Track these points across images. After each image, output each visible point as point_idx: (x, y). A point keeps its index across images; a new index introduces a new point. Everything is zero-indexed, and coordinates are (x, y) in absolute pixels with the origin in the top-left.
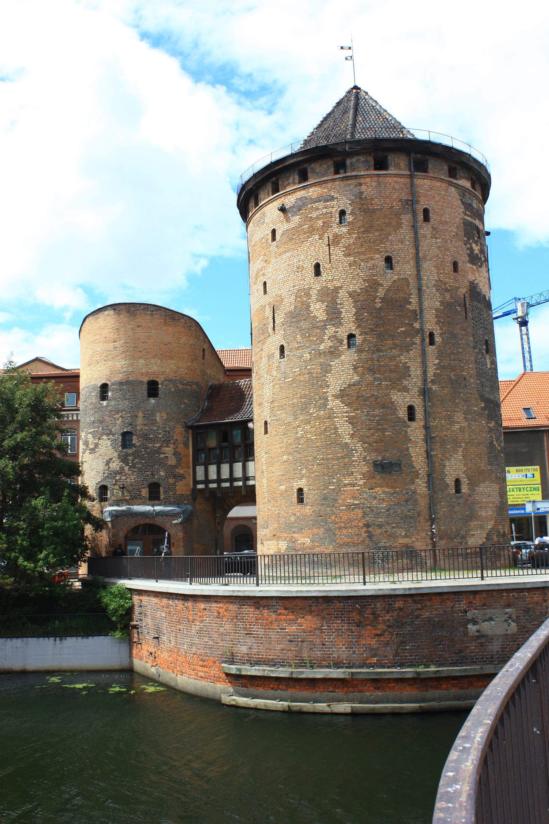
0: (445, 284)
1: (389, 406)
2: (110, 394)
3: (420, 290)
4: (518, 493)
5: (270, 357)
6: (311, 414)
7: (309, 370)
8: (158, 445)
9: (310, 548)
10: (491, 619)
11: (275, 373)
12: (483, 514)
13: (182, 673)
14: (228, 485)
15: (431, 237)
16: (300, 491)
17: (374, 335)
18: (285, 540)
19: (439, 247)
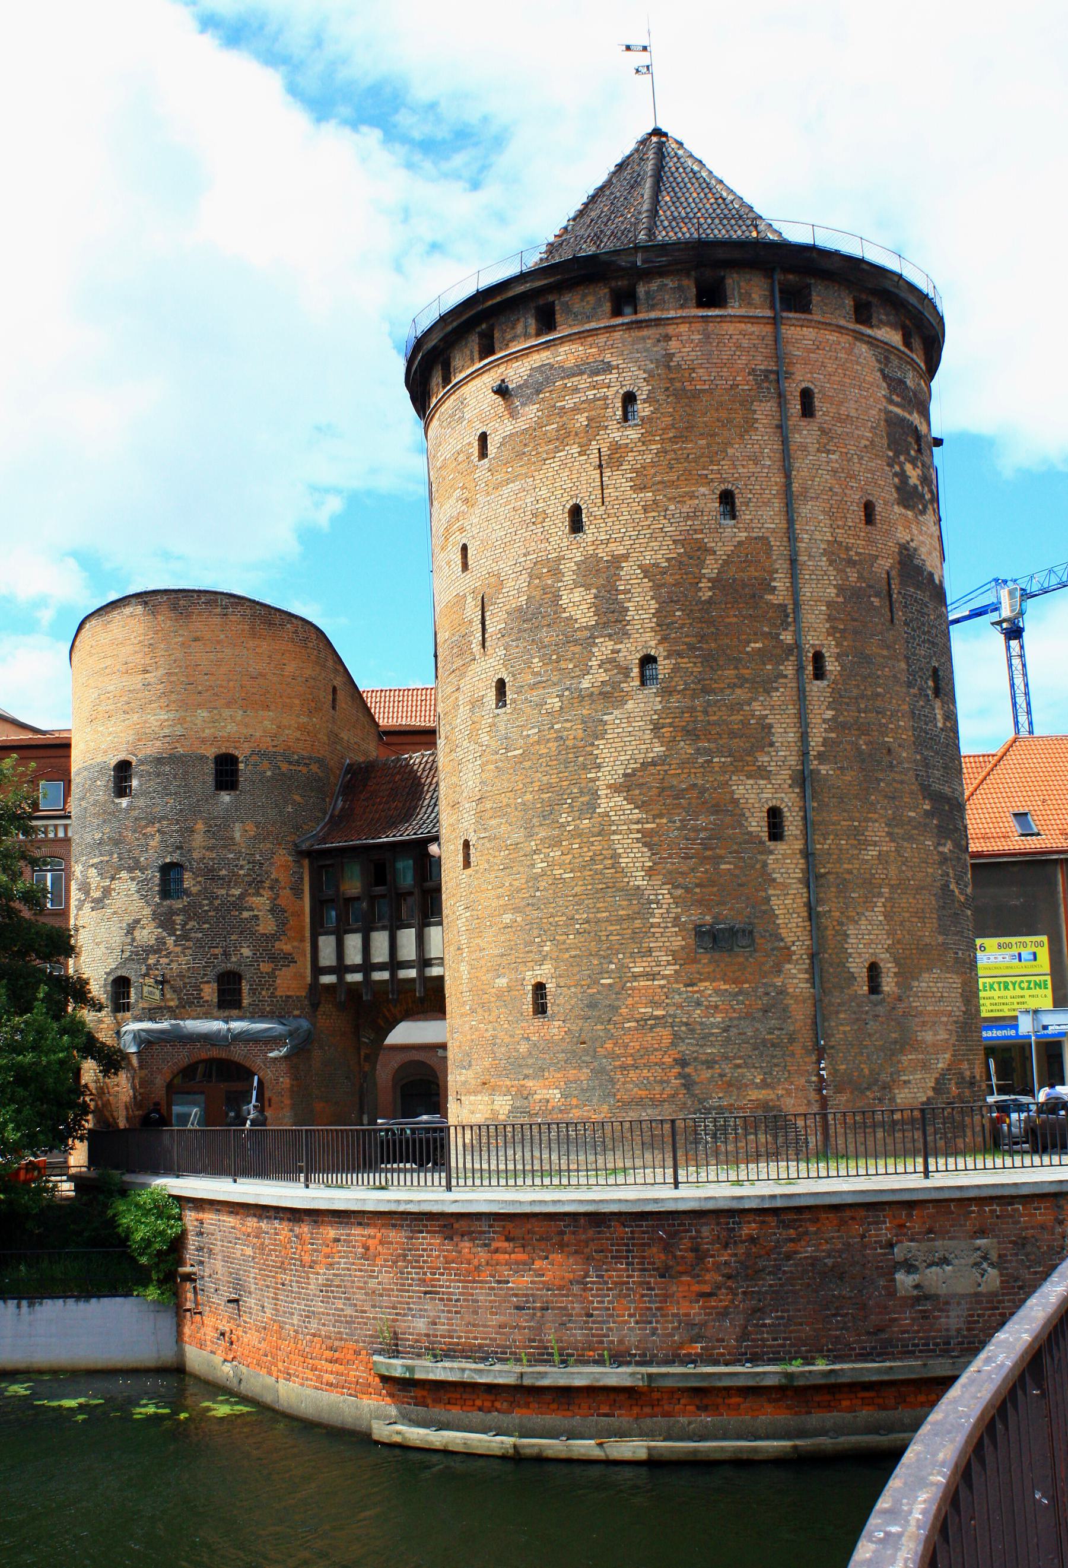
0: (848, 549)
1: (728, 809)
2: (135, 783)
3: (793, 562)
4: (1003, 993)
5: (476, 703)
6: (562, 826)
8: (237, 892)
9: (561, 1111)
10: (945, 1261)
11: (485, 738)
12: (929, 1037)
13: (288, 1376)
14: (385, 975)
15: (818, 450)
16: (539, 988)
17: (696, 657)
18: (508, 1092)
19: (835, 471)
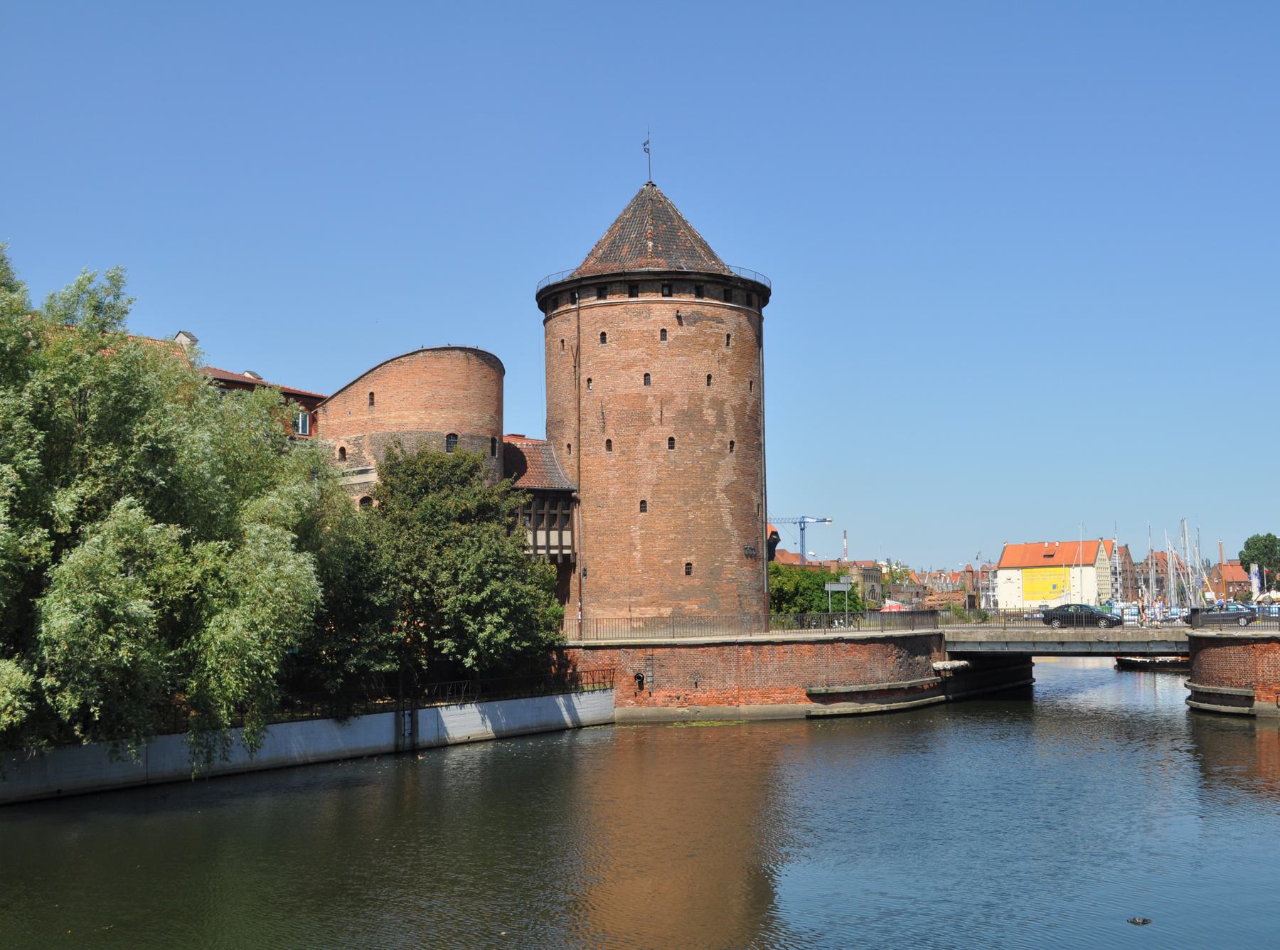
14: (543, 552)
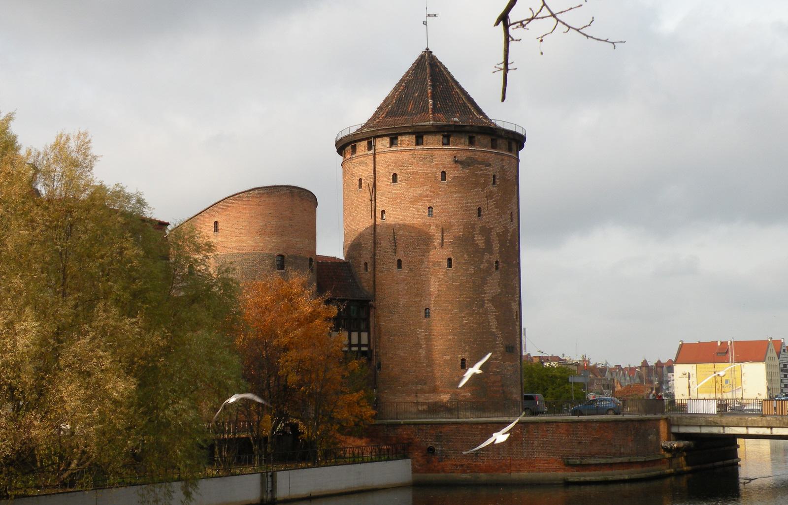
7: (472, 280)
18: (448, 393)
